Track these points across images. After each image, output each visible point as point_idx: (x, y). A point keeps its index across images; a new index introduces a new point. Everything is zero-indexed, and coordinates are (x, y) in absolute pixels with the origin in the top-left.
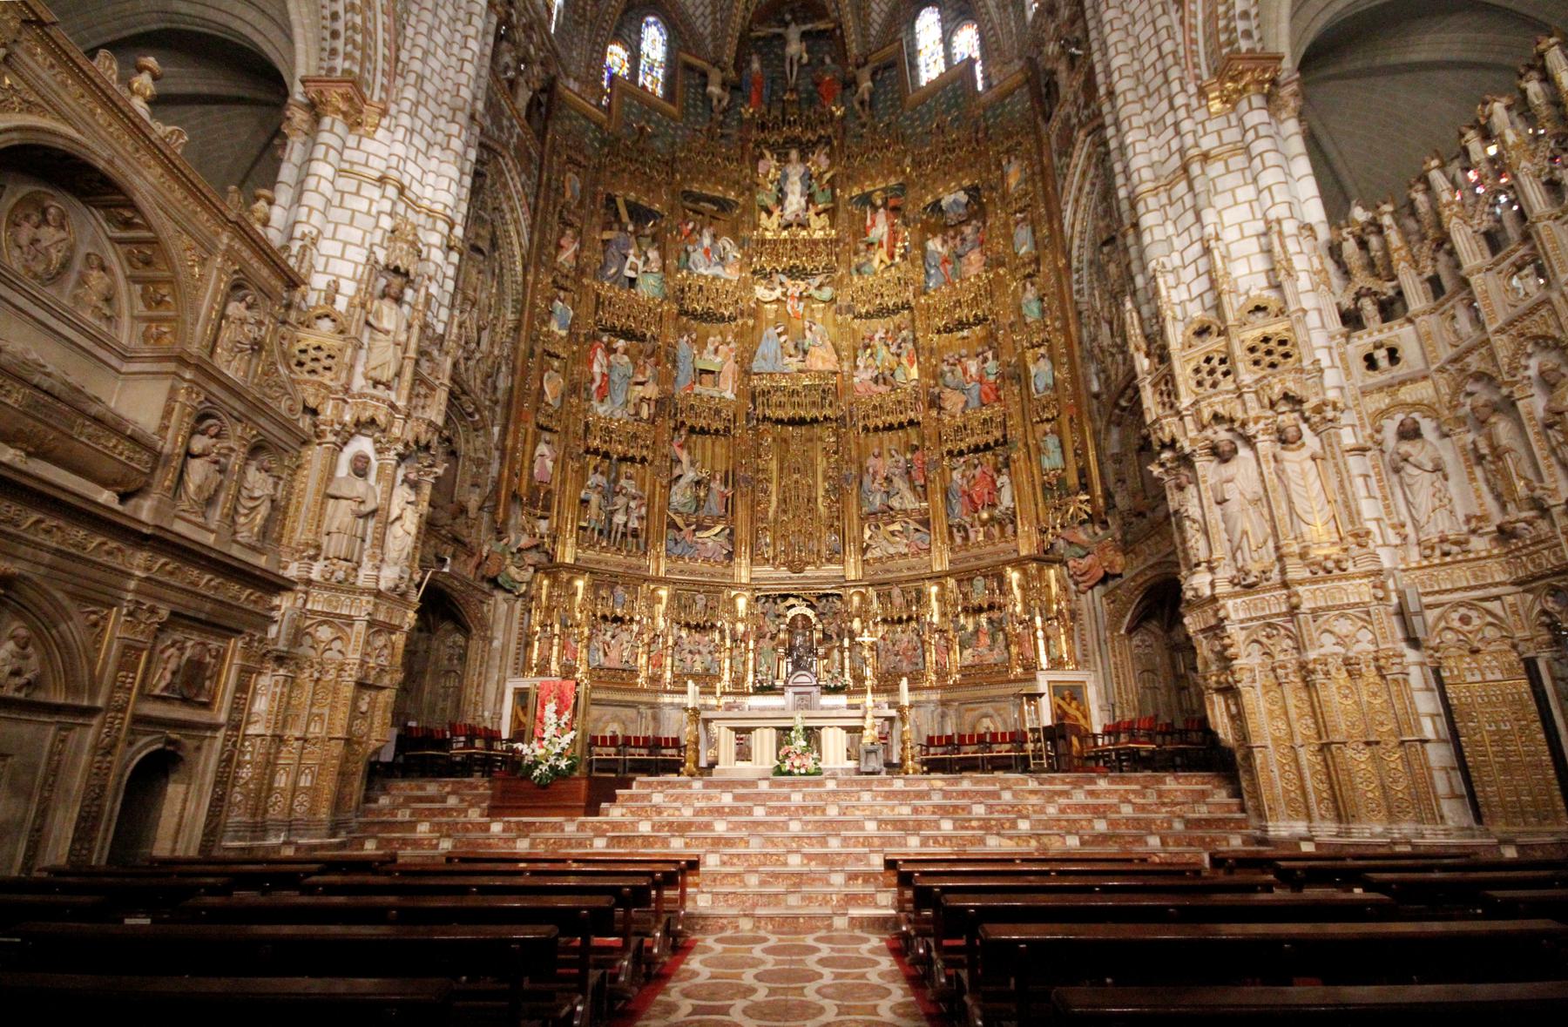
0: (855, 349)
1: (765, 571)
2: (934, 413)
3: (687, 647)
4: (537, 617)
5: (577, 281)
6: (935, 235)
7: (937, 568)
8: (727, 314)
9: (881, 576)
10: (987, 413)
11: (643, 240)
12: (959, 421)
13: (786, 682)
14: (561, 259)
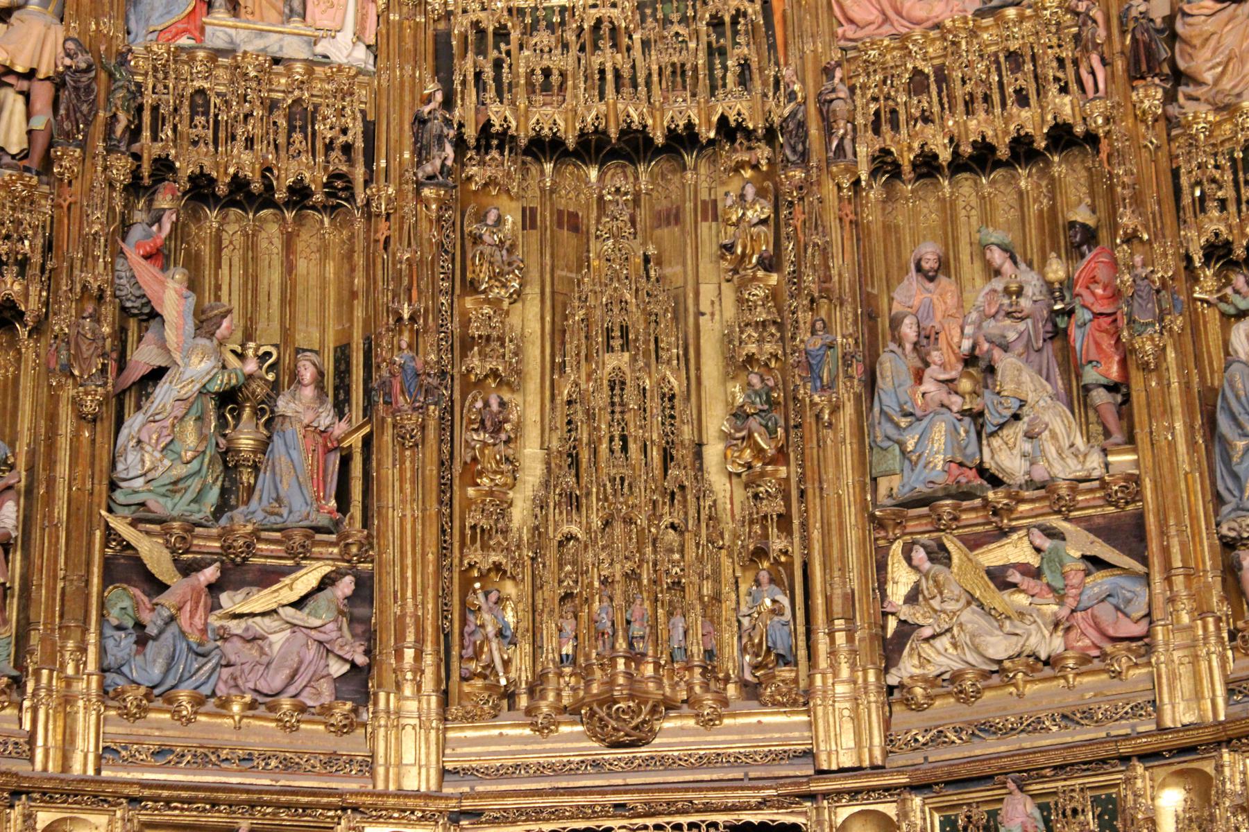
1: (498, 740)
2: (1150, 97)
7: (1178, 713)
9: (957, 752)
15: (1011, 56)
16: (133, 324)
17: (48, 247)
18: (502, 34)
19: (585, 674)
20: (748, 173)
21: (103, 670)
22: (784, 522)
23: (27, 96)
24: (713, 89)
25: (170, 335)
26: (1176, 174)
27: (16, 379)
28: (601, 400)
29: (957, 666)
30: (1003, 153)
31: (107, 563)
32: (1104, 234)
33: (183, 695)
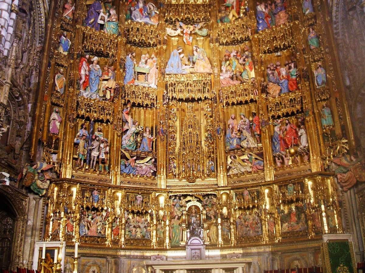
0: (221, 62)
1: (174, 182)
2: (264, 96)
3: (132, 224)
4: (51, 208)
5: (73, 26)
6: (261, 3)
7: (268, 179)
8: (152, 43)
9: (238, 184)
10: (292, 96)
11: (107, 5)
12: (277, 100)
13: (187, 243)
14: (65, 15)
15: (244, 89)
16: (124, 123)
17: (113, 112)
18: (175, 84)
19: (186, 173)
20: (208, 104)
21: (121, 171)
22: (213, 152)
23: (110, 91)
24: (204, 93)
25: (129, 124)
26: (267, 106)
27: (108, 130)
28: (188, 135)
29: (237, 173)
30: (244, 102)
31: (121, 156)
32: (257, 114)
33: (131, 174)
